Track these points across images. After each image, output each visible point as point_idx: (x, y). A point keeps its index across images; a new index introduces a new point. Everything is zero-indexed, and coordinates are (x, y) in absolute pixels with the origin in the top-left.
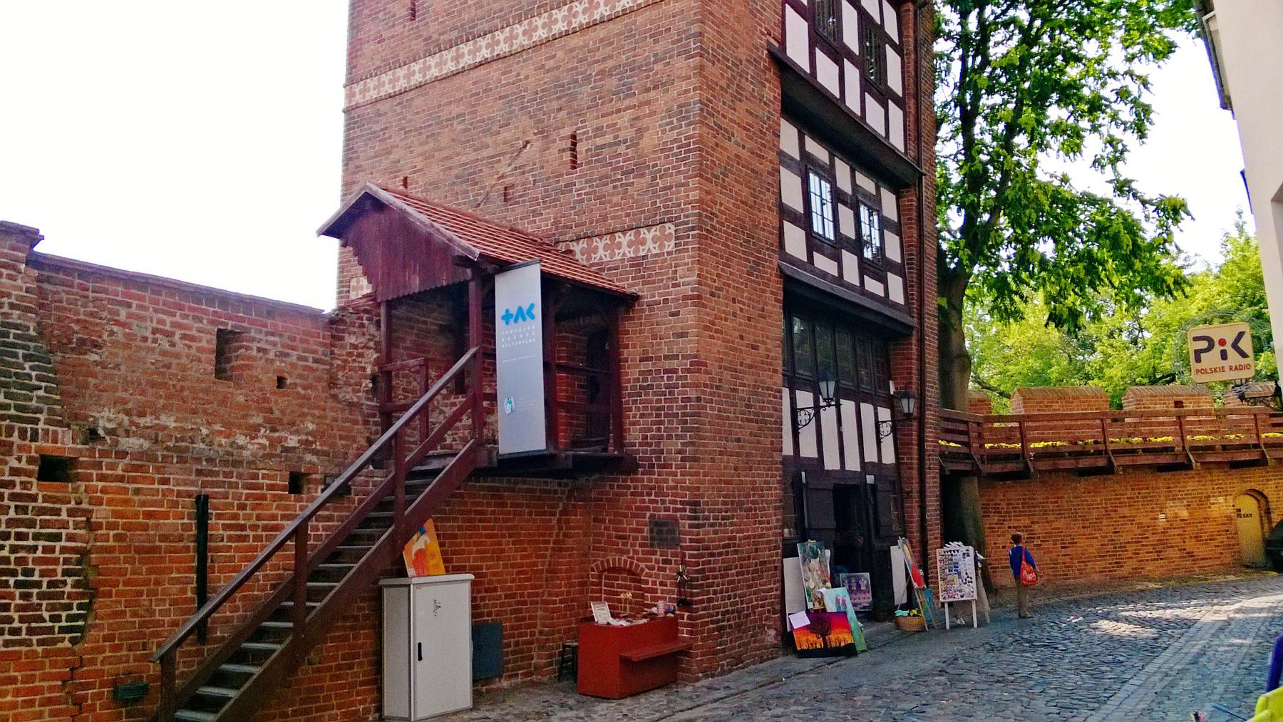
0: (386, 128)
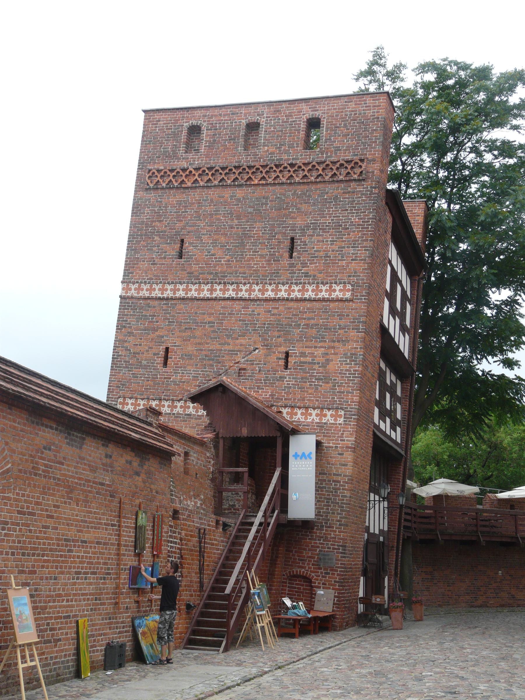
0: (155, 316)
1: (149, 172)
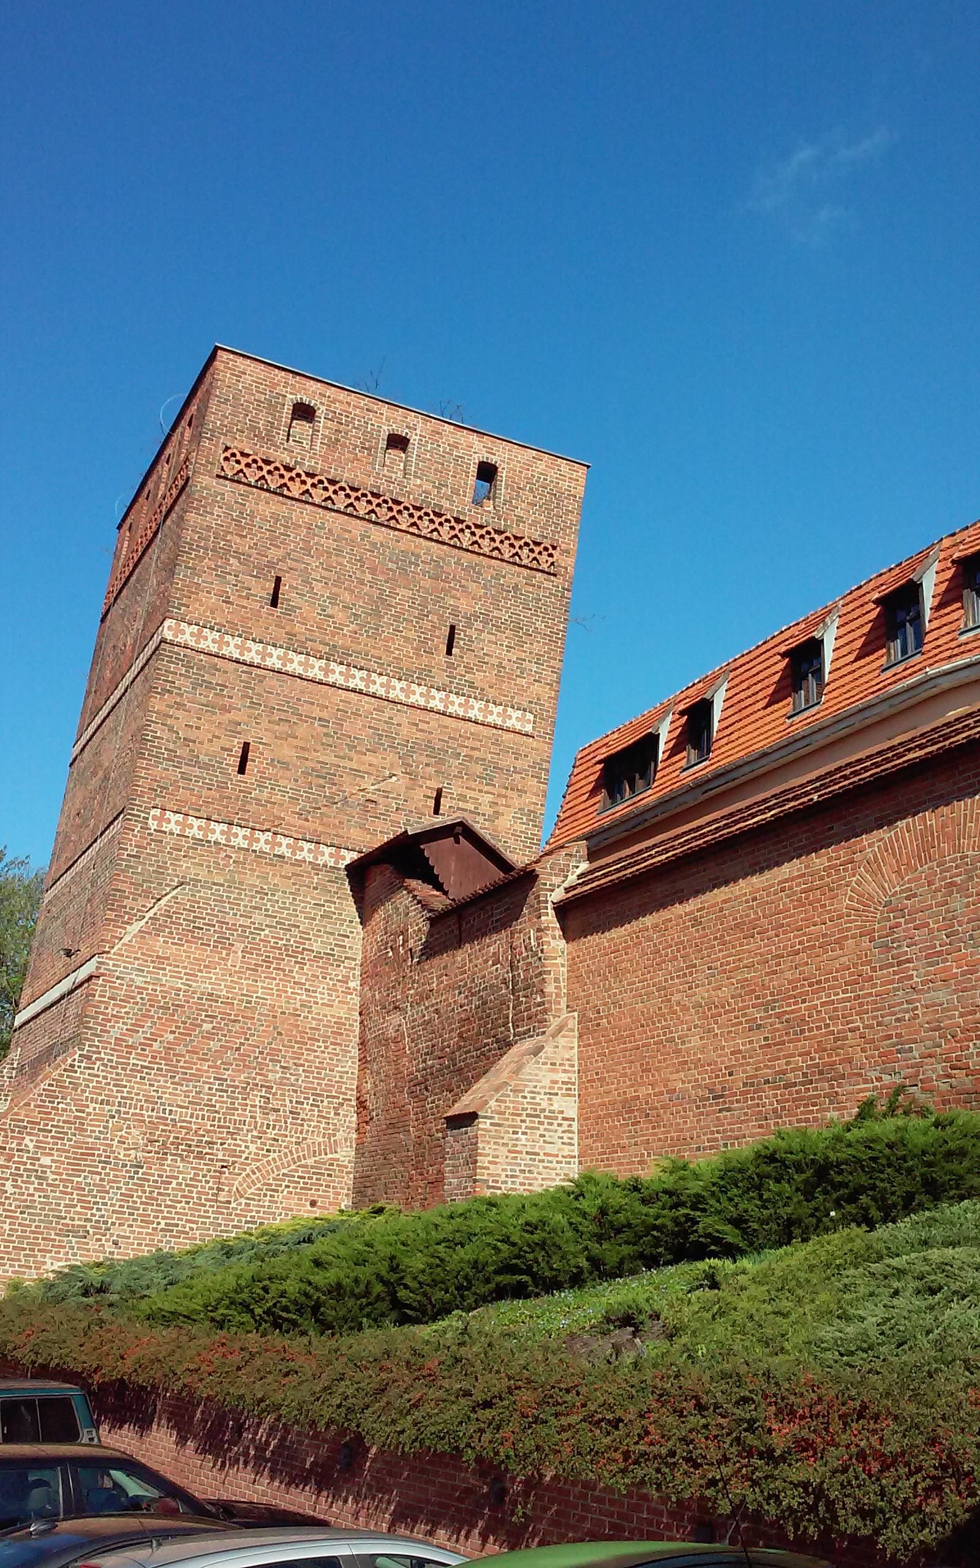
0: (227, 687)
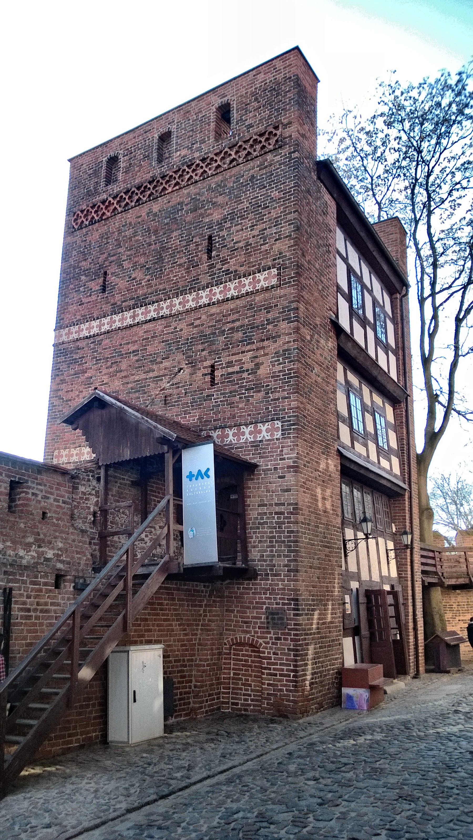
0: (83, 357)
1: (74, 216)
